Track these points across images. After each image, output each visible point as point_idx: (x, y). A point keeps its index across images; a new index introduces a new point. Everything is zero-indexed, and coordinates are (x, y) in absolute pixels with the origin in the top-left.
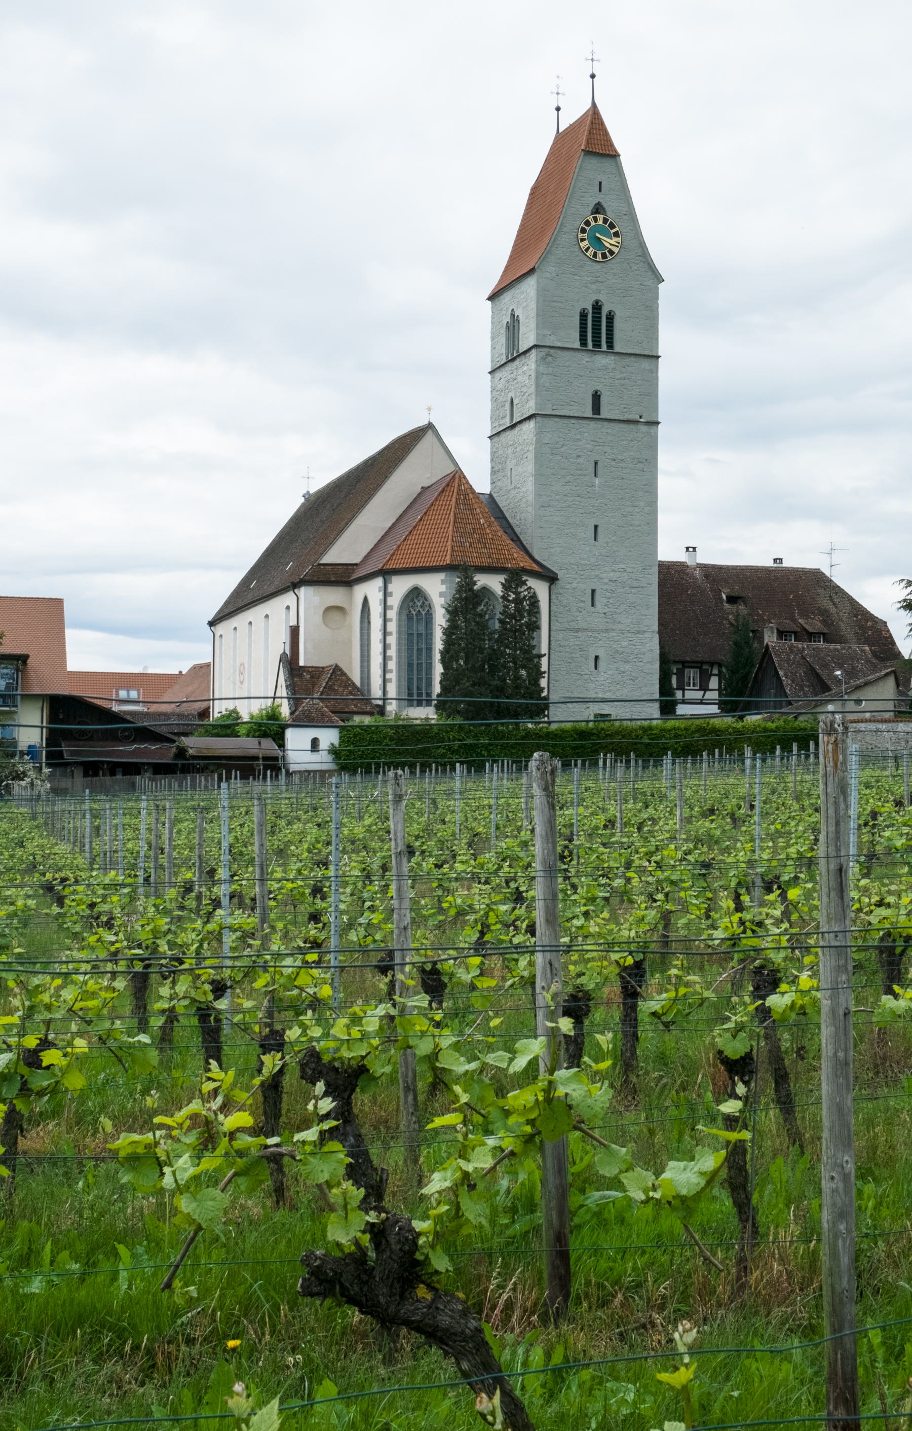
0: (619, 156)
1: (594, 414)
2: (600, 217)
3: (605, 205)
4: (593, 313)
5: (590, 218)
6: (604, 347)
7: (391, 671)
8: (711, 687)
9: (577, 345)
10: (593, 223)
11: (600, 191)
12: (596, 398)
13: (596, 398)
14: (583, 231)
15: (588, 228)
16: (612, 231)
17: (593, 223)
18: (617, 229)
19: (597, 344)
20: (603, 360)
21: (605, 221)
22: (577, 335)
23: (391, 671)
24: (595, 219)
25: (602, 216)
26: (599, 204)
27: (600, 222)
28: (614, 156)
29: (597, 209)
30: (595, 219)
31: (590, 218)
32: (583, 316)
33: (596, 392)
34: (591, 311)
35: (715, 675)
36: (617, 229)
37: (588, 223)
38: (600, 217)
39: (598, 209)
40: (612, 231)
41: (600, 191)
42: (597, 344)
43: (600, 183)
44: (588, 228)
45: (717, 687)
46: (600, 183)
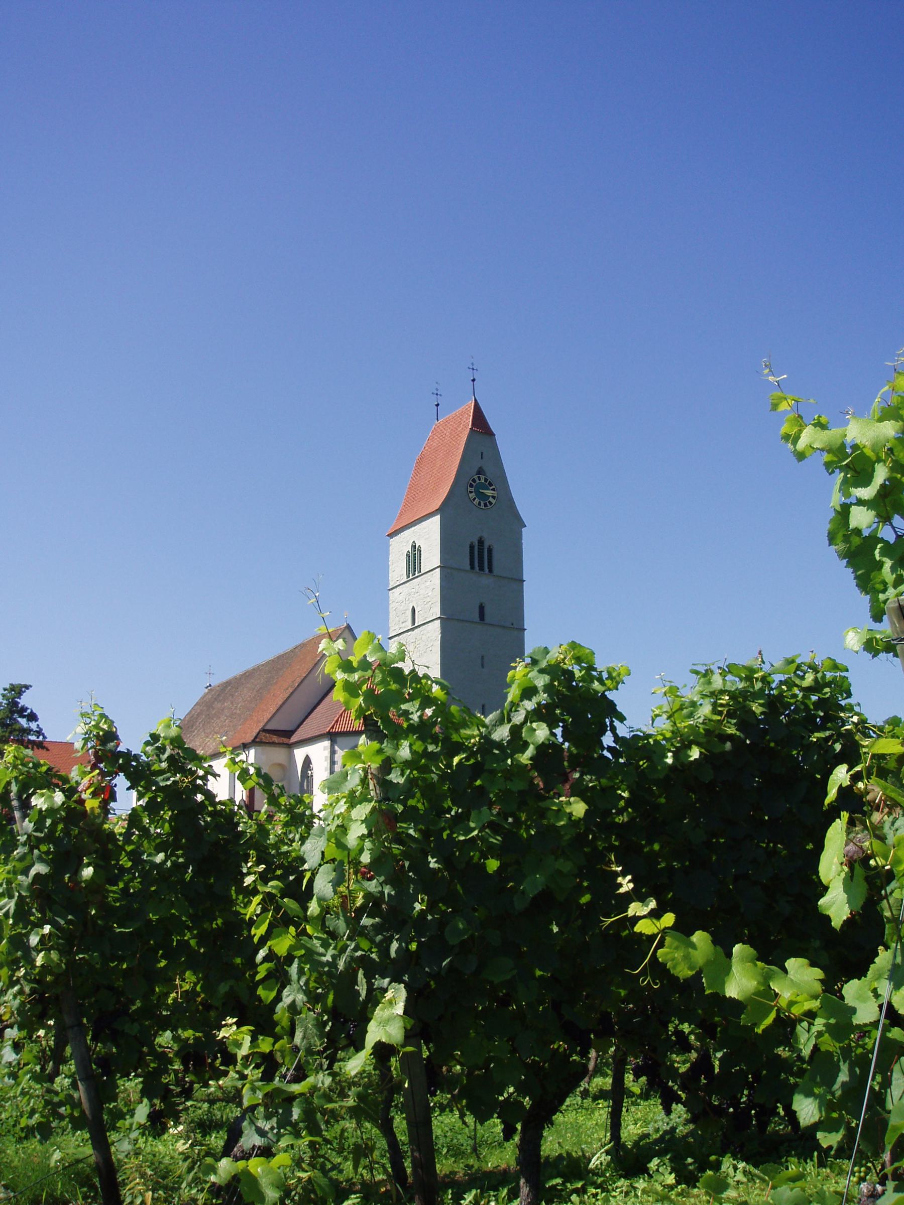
0: (494, 435)
2: (483, 477)
3: (484, 468)
5: (476, 477)
10: (478, 481)
12: (482, 609)
13: (482, 609)
14: (471, 486)
17: (478, 481)
19: (481, 568)
20: (485, 580)
21: (486, 480)
26: (480, 468)
28: (491, 434)
31: (476, 477)
32: (472, 547)
37: (474, 481)
38: (483, 477)
39: (480, 472)
42: (481, 568)
43: (482, 453)
46: (482, 453)
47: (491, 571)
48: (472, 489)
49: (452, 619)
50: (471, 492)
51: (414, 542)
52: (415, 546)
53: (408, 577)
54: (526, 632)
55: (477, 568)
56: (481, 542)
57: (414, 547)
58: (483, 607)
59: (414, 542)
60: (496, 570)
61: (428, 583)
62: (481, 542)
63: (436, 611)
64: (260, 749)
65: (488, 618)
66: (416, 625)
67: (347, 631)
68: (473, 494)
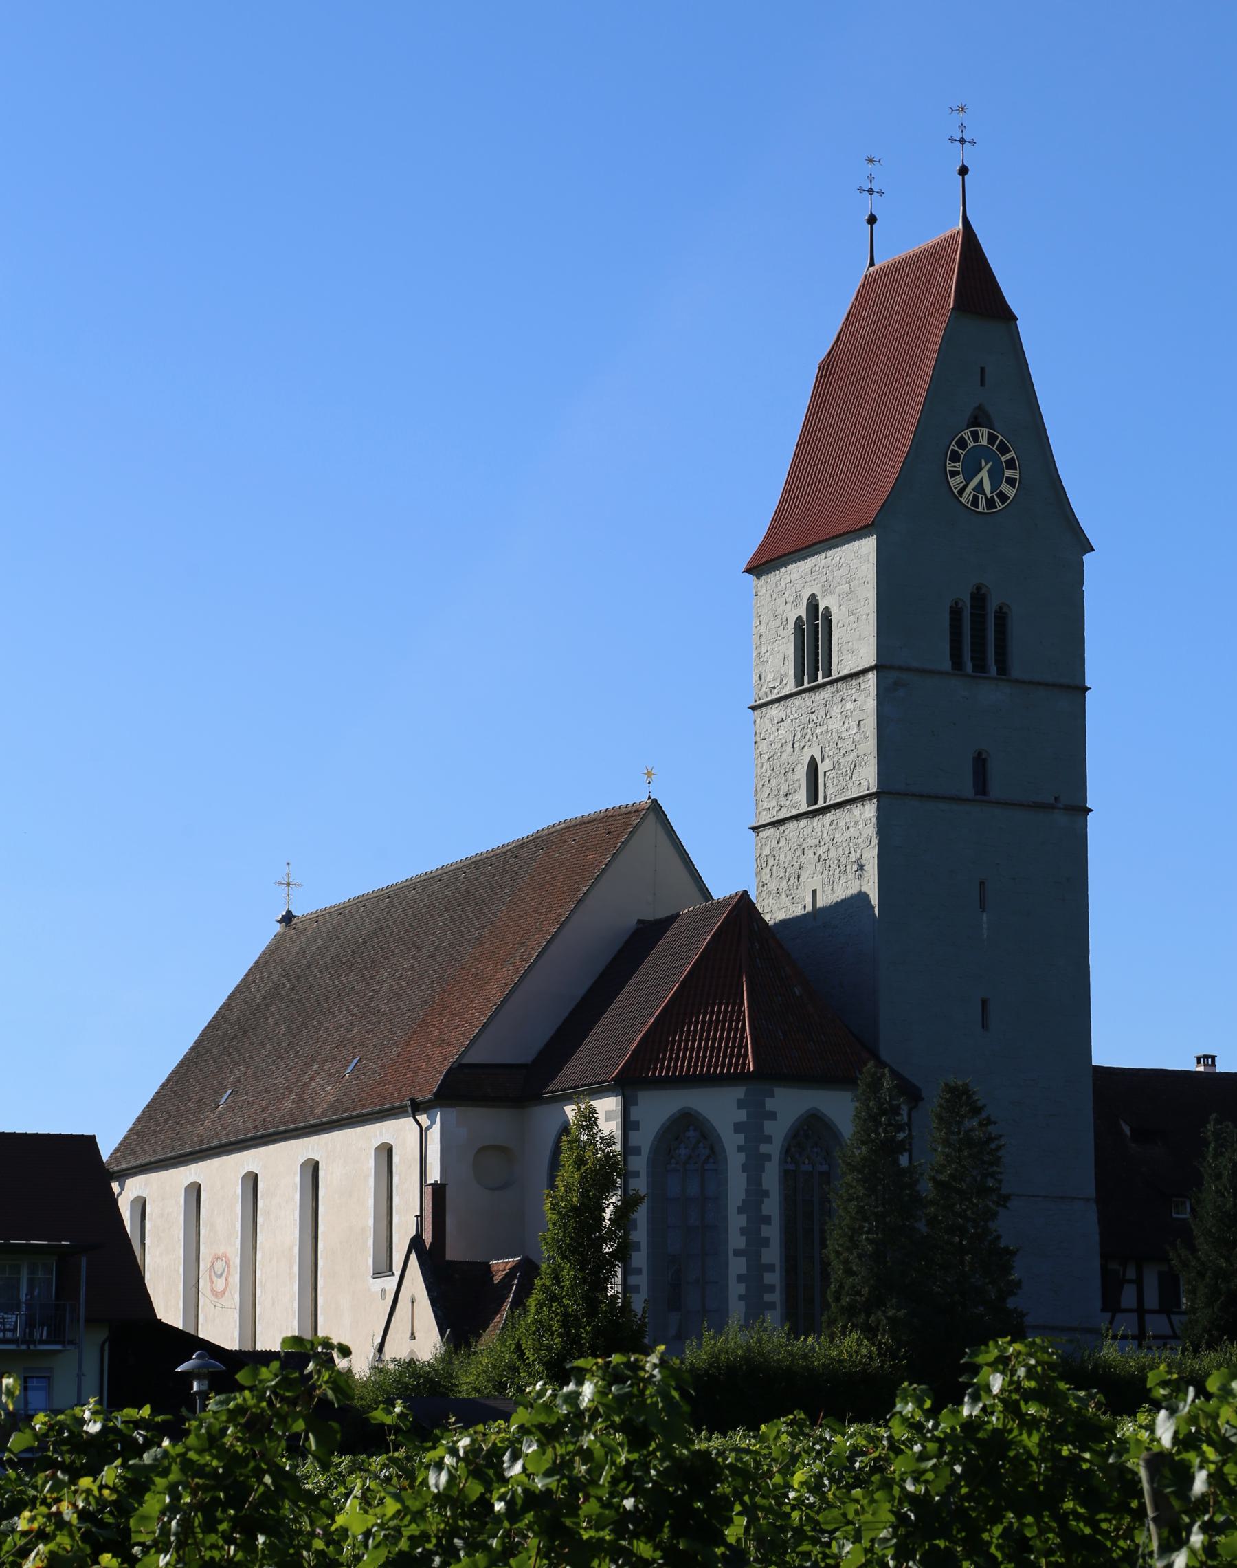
0: (1017, 319)
1: (976, 794)
2: (984, 432)
4: (972, 607)
5: (966, 434)
6: (993, 670)
7: (638, 1271)
8: (1124, 1305)
9: (947, 665)
10: (971, 444)
11: (982, 383)
12: (980, 763)
13: (980, 763)
14: (955, 457)
15: (962, 453)
16: (1004, 459)
17: (971, 444)
18: (1012, 454)
19: (980, 667)
21: (992, 439)
22: (946, 647)
23: (638, 1271)
24: (975, 436)
25: (986, 430)
27: (984, 441)
28: (1009, 317)
29: (976, 418)
30: (975, 436)
31: (966, 434)
32: (956, 613)
33: (980, 754)
34: (969, 605)
35: (1130, 1281)
36: (1012, 454)
37: (962, 443)
38: (984, 432)
40: (1004, 459)
41: (982, 383)
42: (980, 667)
43: (983, 370)
44: (962, 453)
45: (1134, 1305)
46: (983, 370)
47: (1003, 669)
48: (958, 466)
49: (906, 795)
50: (954, 474)
51: (813, 596)
52: (817, 607)
53: (800, 682)
54: (1090, 816)
55: (969, 667)
56: (979, 598)
57: (813, 605)
58: (984, 760)
59: (813, 596)
60: (1016, 672)
61: (849, 706)
62: (979, 598)
63: (868, 777)
64: (453, 1113)
65: (996, 791)
66: (821, 804)
67: (651, 817)
68: (960, 478)
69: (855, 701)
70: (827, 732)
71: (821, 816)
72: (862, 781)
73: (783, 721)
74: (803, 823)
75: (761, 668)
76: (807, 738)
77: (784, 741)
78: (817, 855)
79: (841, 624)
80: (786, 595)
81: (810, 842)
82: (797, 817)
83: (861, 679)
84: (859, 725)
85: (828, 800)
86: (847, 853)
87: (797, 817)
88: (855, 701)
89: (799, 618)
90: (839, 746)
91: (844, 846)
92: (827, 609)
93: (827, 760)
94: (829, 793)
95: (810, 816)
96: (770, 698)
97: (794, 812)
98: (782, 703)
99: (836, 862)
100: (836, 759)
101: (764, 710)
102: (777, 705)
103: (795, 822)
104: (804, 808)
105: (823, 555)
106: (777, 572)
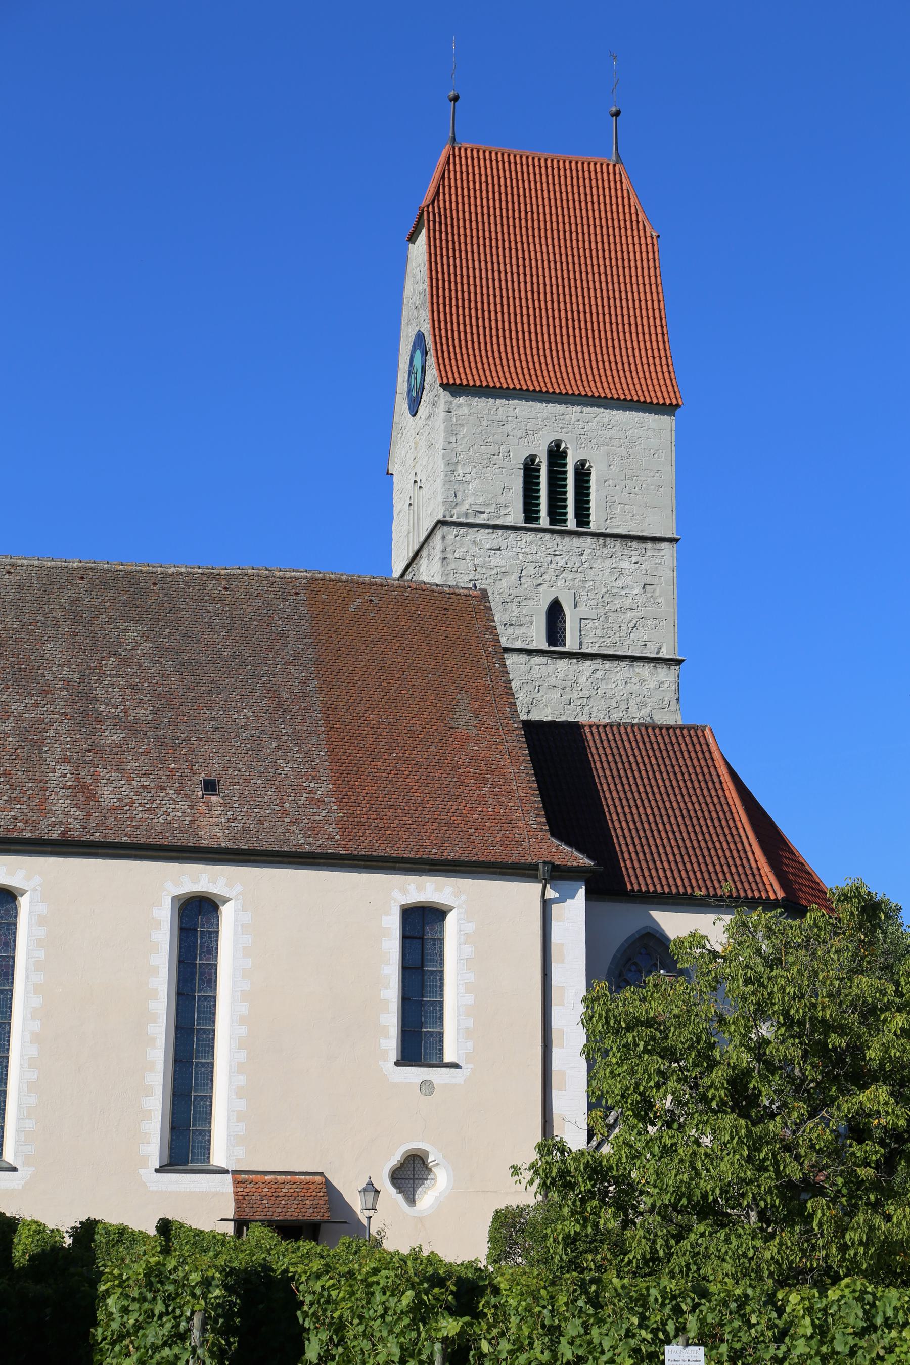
69: (637, 563)
70: (585, 581)
71: (575, 661)
72: (648, 643)
73: (499, 549)
74: (537, 660)
75: (460, 488)
76: (547, 577)
77: (503, 570)
78: (566, 697)
79: (611, 482)
80: (508, 427)
81: (553, 681)
82: (531, 652)
83: (649, 545)
84: (644, 588)
85: (584, 647)
86: (623, 707)
87: (531, 652)
88: (637, 563)
89: (532, 458)
90: (606, 599)
91: (619, 698)
92: (583, 463)
93: (583, 610)
94: (585, 641)
95: (556, 656)
96: (471, 520)
97: (518, 644)
98: (500, 532)
99: (603, 712)
100: (601, 611)
101: (463, 530)
102: (487, 531)
103: (525, 656)
104: (545, 646)
105: (579, 409)
106: (491, 401)
